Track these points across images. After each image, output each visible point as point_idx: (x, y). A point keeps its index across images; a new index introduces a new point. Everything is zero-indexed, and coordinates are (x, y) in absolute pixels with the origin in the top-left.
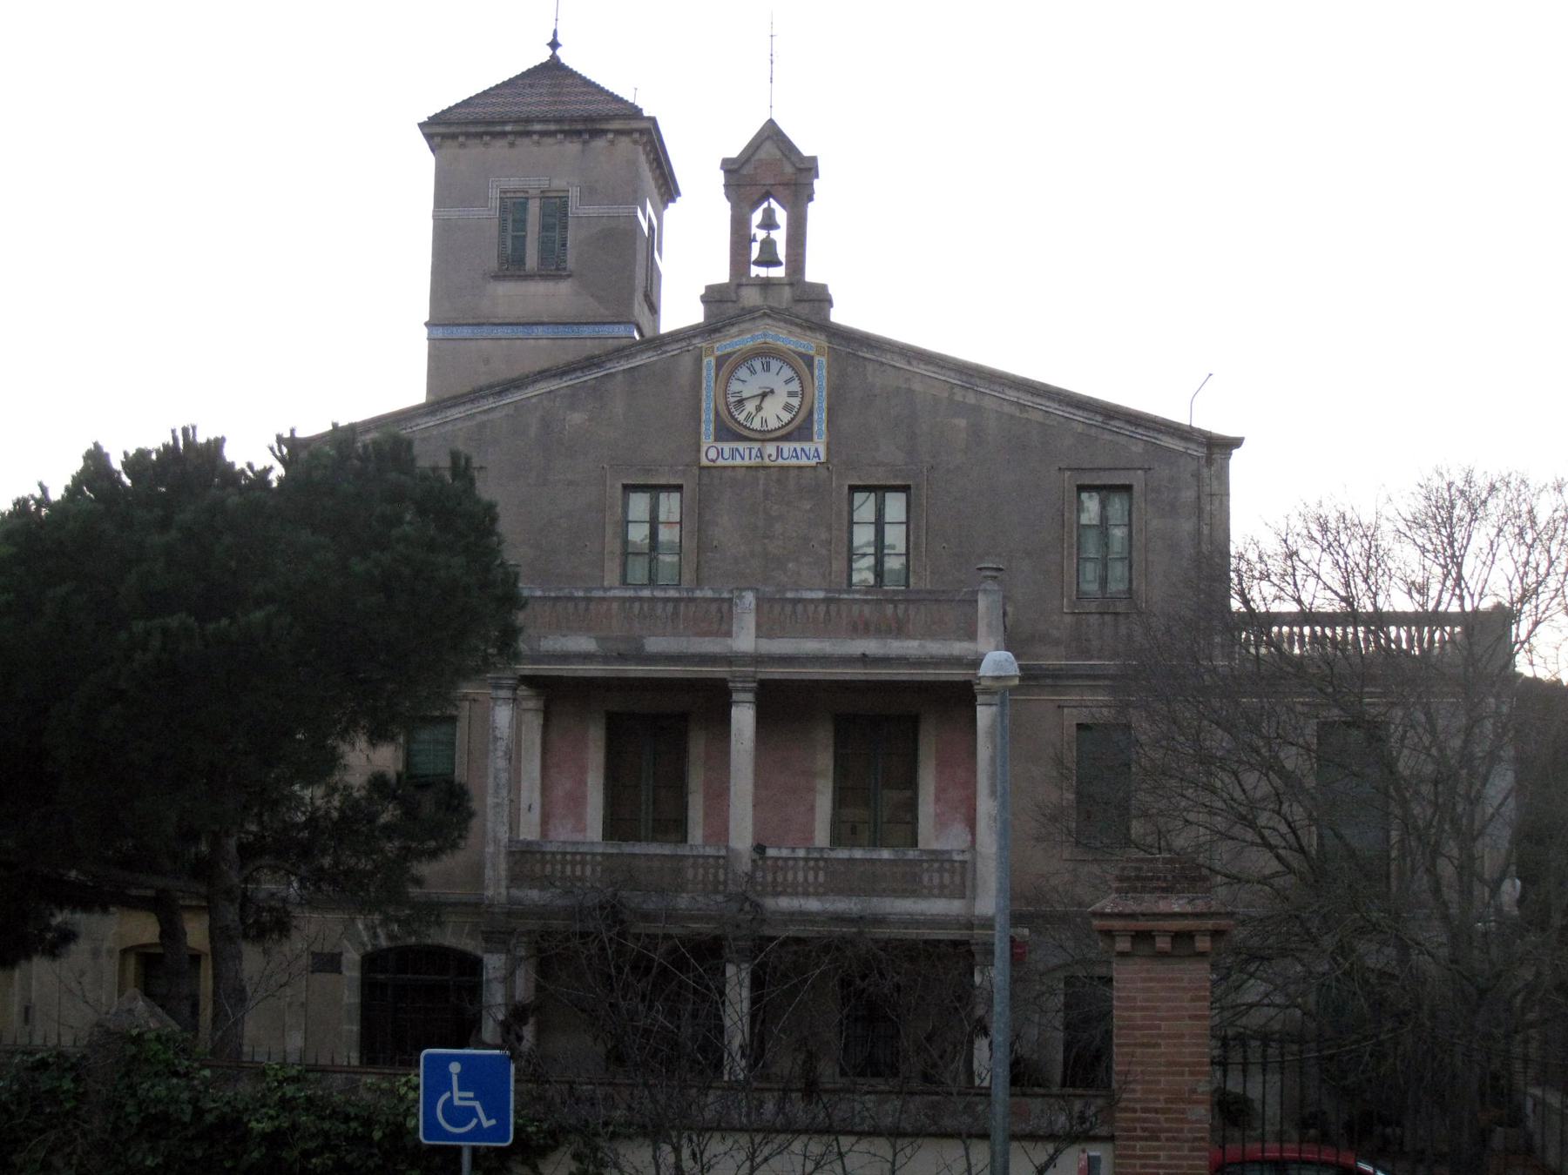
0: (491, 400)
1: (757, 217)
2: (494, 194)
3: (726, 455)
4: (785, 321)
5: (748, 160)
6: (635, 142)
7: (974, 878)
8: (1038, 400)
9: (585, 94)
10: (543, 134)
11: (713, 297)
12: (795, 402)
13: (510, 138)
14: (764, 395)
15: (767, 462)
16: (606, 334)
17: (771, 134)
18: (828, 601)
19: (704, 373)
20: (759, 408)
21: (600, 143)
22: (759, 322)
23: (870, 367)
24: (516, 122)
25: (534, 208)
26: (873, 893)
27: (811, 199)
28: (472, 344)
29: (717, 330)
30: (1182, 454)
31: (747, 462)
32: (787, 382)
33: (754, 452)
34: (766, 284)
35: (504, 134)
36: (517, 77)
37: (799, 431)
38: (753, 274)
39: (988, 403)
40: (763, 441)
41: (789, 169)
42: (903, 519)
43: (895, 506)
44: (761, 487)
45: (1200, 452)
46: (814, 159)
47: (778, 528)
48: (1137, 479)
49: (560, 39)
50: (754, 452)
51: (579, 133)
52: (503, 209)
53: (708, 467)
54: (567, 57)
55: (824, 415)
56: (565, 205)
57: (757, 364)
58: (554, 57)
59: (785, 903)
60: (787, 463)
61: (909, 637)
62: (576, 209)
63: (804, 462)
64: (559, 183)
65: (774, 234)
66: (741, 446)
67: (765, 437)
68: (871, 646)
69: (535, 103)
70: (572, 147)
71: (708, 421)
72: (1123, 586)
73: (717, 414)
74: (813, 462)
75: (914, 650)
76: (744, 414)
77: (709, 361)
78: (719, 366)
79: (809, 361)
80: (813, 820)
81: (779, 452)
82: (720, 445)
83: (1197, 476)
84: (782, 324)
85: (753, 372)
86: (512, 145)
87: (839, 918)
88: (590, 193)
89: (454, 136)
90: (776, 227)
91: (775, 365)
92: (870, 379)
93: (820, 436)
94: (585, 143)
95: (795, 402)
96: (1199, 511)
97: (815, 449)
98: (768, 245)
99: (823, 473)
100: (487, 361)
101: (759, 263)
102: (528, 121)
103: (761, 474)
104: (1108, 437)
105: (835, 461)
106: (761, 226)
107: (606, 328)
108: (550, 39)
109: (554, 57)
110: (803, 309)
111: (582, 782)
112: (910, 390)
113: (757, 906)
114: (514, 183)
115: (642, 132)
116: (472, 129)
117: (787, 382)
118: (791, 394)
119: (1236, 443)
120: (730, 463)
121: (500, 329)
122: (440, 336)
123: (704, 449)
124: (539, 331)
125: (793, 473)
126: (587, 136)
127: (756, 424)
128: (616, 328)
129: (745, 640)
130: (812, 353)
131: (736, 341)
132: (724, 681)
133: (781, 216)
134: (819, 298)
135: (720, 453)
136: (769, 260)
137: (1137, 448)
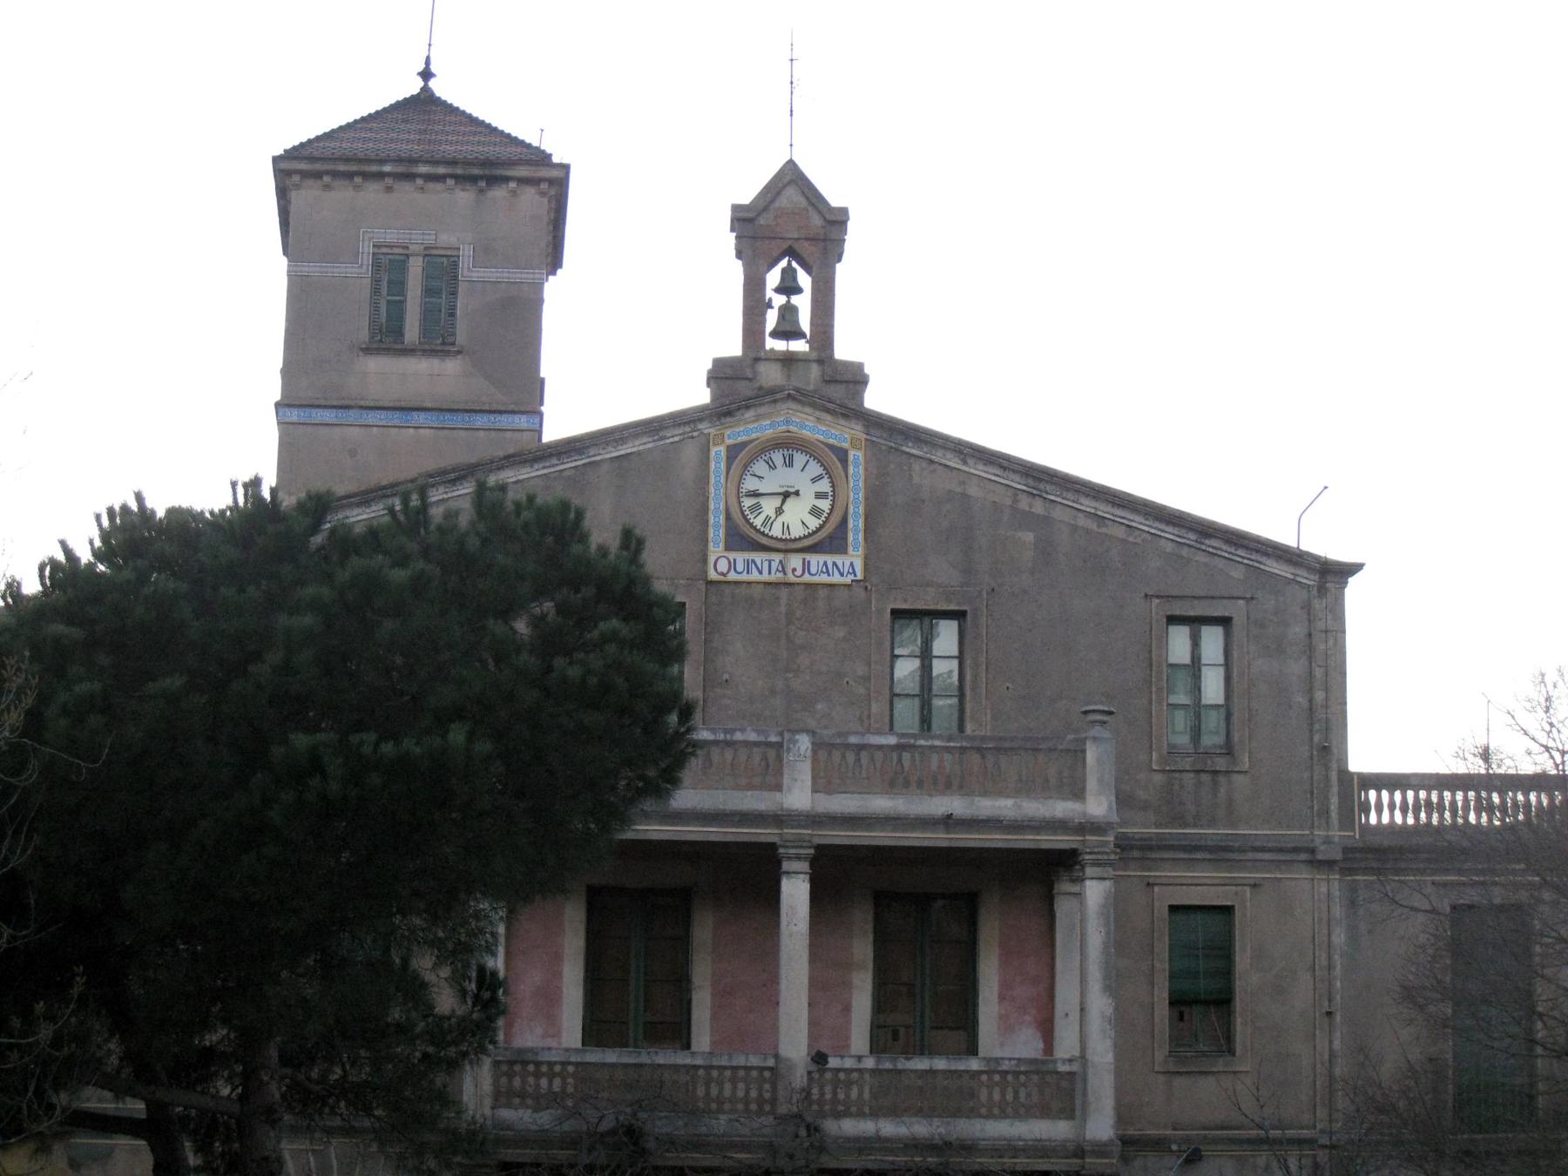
0: (441, 489)
1: (773, 278)
2: (367, 249)
3: (740, 567)
4: (814, 406)
5: (765, 209)
6: (543, 194)
7: (1085, 1094)
8: (1119, 512)
9: (475, 134)
10: (430, 178)
11: (722, 374)
12: (825, 505)
13: (389, 181)
14: (786, 495)
15: (791, 578)
17: (791, 178)
18: (900, 748)
19: (713, 465)
20: (779, 511)
21: (499, 193)
22: (779, 406)
23: (916, 467)
24: (399, 160)
25: (416, 267)
26: (957, 1113)
27: (839, 260)
28: (337, 430)
29: (729, 414)
30: (1289, 582)
31: (765, 577)
32: (814, 480)
33: (774, 565)
34: (788, 359)
35: (380, 176)
36: (385, 109)
37: (831, 540)
38: (768, 347)
39: (1057, 513)
40: (786, 551)
41: (817, 221)
42: (955, 652)
43: (946, 638)
44: (783, 609)
45: (1310, 580)
46: (844, 212)
47: (804, 660)
48: (1237, 610)
49: (433, 68)
50: (774, 565)
51: (474, 179)
52: (377, 265)
53: (719, 582)
54: (439, 88)
55: (861, 525)
56: (456, 264)
57: (777, 457)
58: (425, 89)
59: (851, 1127)
60: (816, 579)
61: (1001, 793)
62: (468, 270)
63: (836, 578)
64: (446, 239)
65: (795, 300)
66: (758, 557)
67: (788, 546)
68: (954, 805)
69: (406, 142)
70: (464, 197)
71: (717, 525)
72: (1219, 739)
73: (728, 517)
74: (848, 579)
75: (1005, 810)
76: (761, 518)
77: (718, 452)
78: (730, 459)
79: (842, 455)
80: (849, 1022)
81: (806, 566)
82: (732, 555)
83: (1308, 607)
84: (808, 410)
85: (773, 467)
86: (389, 189)
87: (913, 1145)
88: (485, 253)
89: (318, 175)
90: (799, 290)
91: (799, 459)
92: (916, 479)
93: (856, 548)
95: (825, 505)
96: (1310, 651)
97: (850, 564)
98: (788, 312)
99: (859, 593)
100: (353, 453)
101: (776, 334)
102: (413, 161)
103: (784, 592)
104: (1201, 558)
105: (874, 579)
106: (778, 290)
108: (422, 67)
109: (425, 89)
110: (836, 392)
111: (558, 975)
112: (964, 495)
113: (813, 1129)
114: (391, 237)
115: (551, 182)
116: (342, 167)
117: (814, 480)
118: (819, 496)
119: (1354, 569)
120: (744, 577)
121: (372, 414)
122: (295, 419)
123: (712, 559)
124: (420, 418)
125: (822, 593)
126: (483, 184)
127: (776, 531)
128: (517, 418)
129: (799, 795)
130: (845, 445)
131: (754, 428)
132: (772, 847)
133: (804, 280)
134: (854, 378)
135: (732, 565)
136: (788, 330)
137: (1237, 573)
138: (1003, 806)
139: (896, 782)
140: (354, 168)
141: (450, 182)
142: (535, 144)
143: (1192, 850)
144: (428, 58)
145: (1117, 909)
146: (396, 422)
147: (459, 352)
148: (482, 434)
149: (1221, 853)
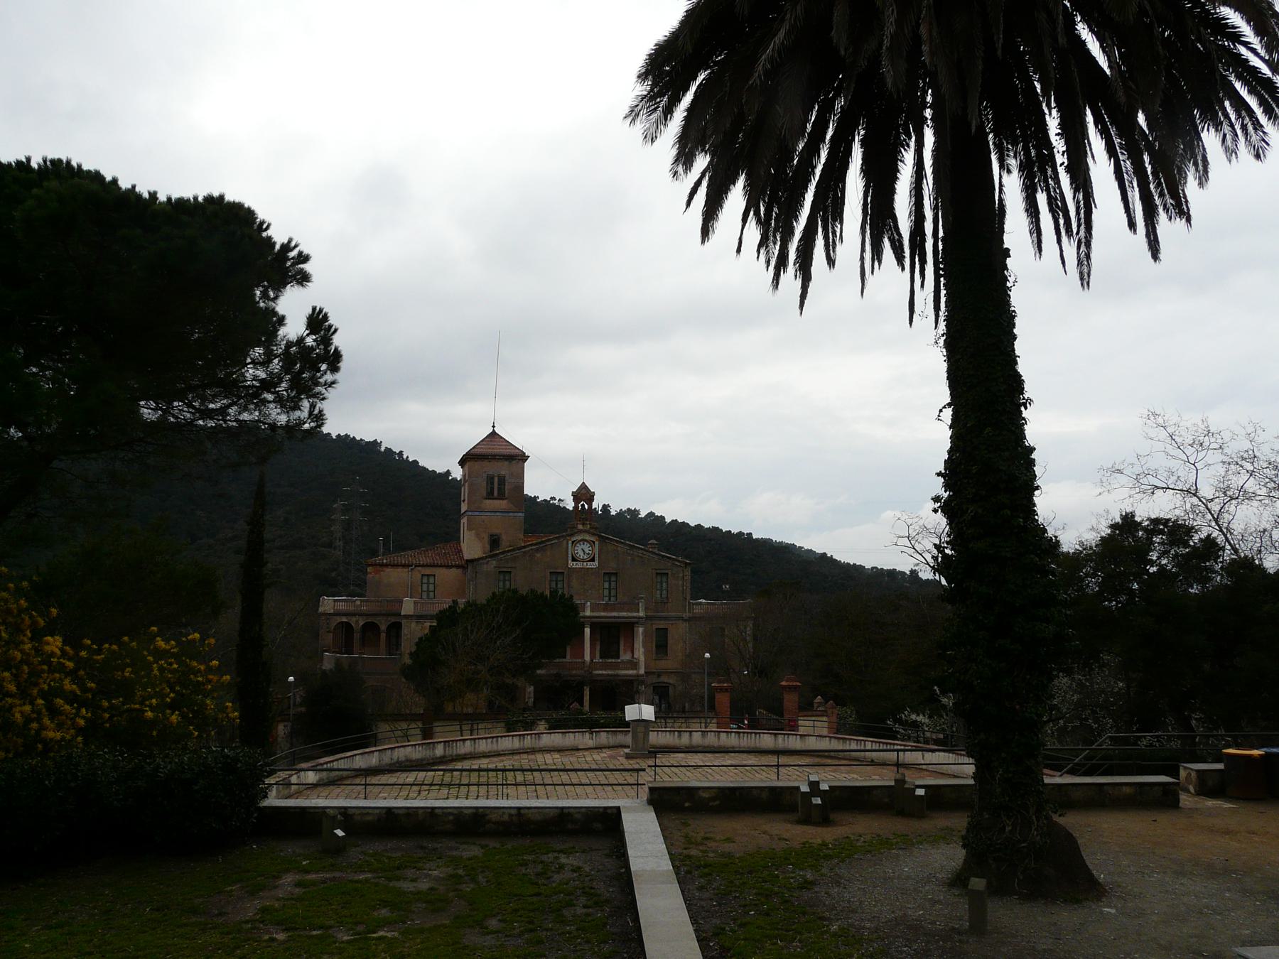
67: (583, 560)
97: (596, 563)
138: (624, 614)
139: (604, 611)
143: (661, 618)
145: (645, 634)
149: (666, 618)
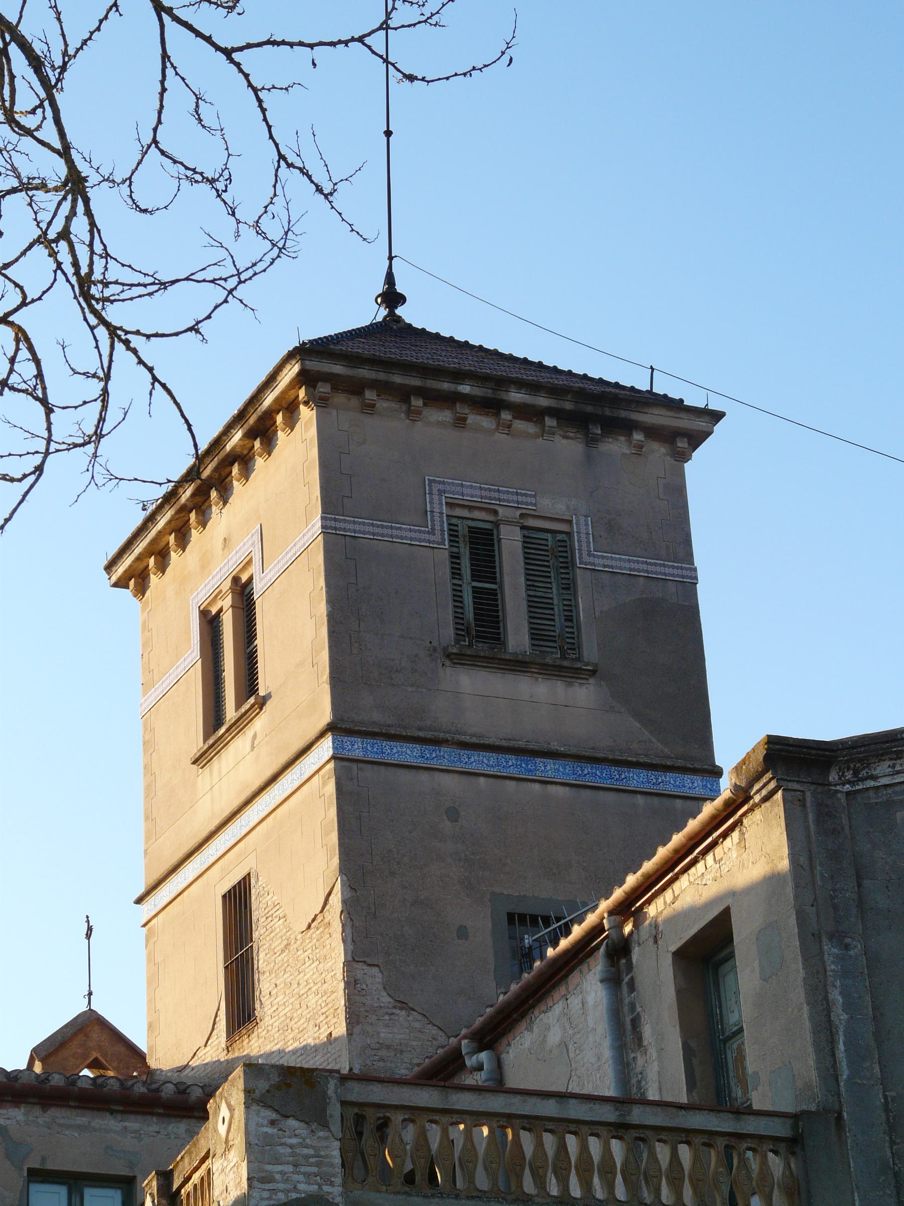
2: (438, 507)
16: (670, 789)
21: (615, 447)
28: (424, 776)
49: (399, 288)
52: (453, 534)
58: (393, 319)
64: (552, 505)
70: (567, 448)
86: (460, 422)
94: (591, 441)
100: (453, 814)
102: (502, 383)
107: (670, 777)
114: (471, 493)
116: (398, 379)
122: (358, 754)
124: (549, 768)
128: (687, 779)
140: (416, 382)
141: (550, 422)
142: (644, 386)
144: (390, 279)
146: (513, 772)
147: (593, 673)
148: (640, 800)
